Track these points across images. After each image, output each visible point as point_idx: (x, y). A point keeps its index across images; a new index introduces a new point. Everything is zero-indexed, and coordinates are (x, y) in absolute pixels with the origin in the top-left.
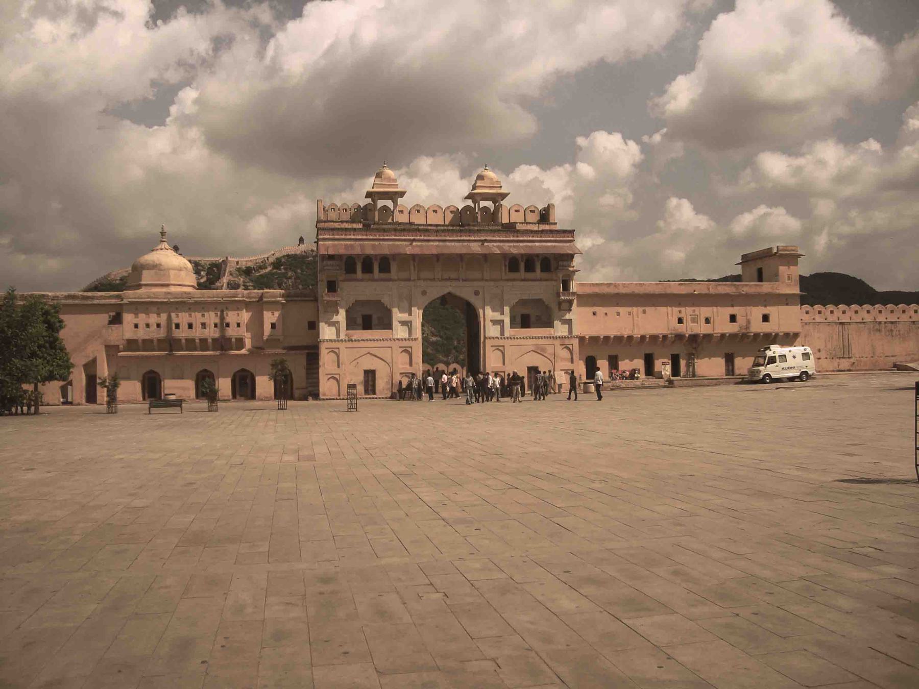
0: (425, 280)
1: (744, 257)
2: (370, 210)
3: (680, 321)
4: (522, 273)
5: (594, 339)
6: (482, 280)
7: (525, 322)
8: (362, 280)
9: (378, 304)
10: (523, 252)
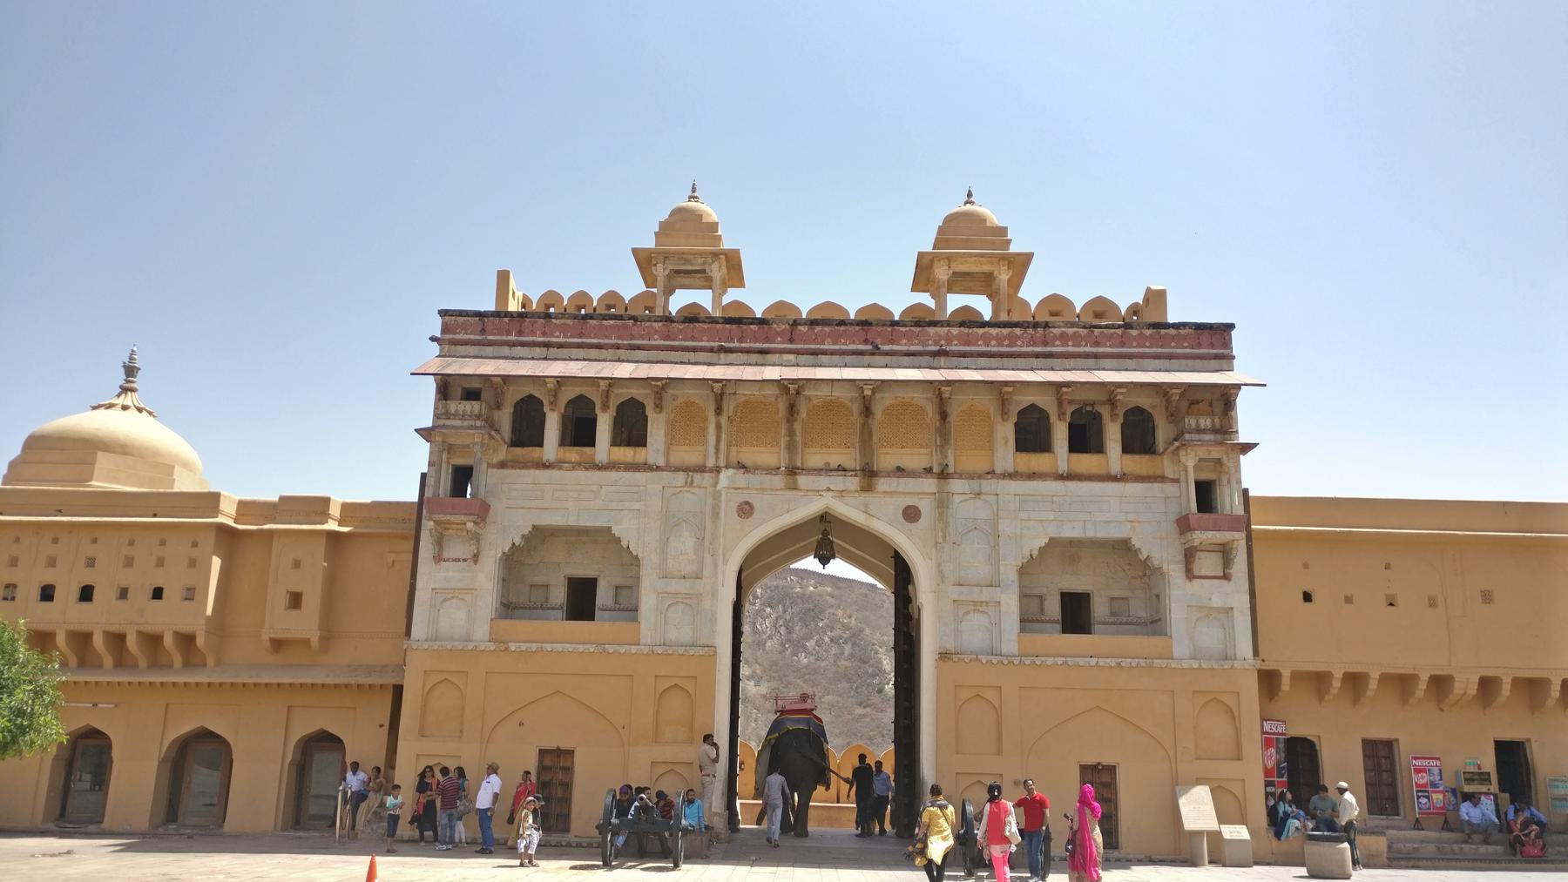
7: (1076, 614)
9: (603, 538)
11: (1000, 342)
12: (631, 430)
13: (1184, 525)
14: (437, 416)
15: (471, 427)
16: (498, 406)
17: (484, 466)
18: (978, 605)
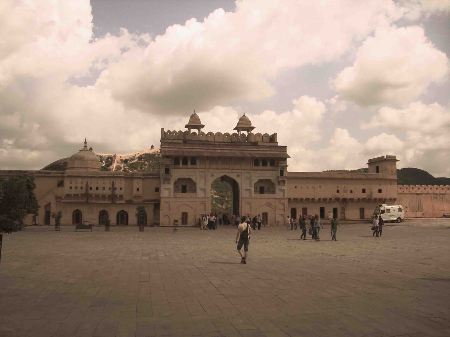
0: (213, 169)
1: (369, 160)
2: (187, 134)
3: (338, 192)
4: (261, 167)
5: (296, 200)
6: (241, 169)
7: (262, 191)
9: (190, 180)
10: (261, 156)
13: (278, 177)
18: (247, 190)
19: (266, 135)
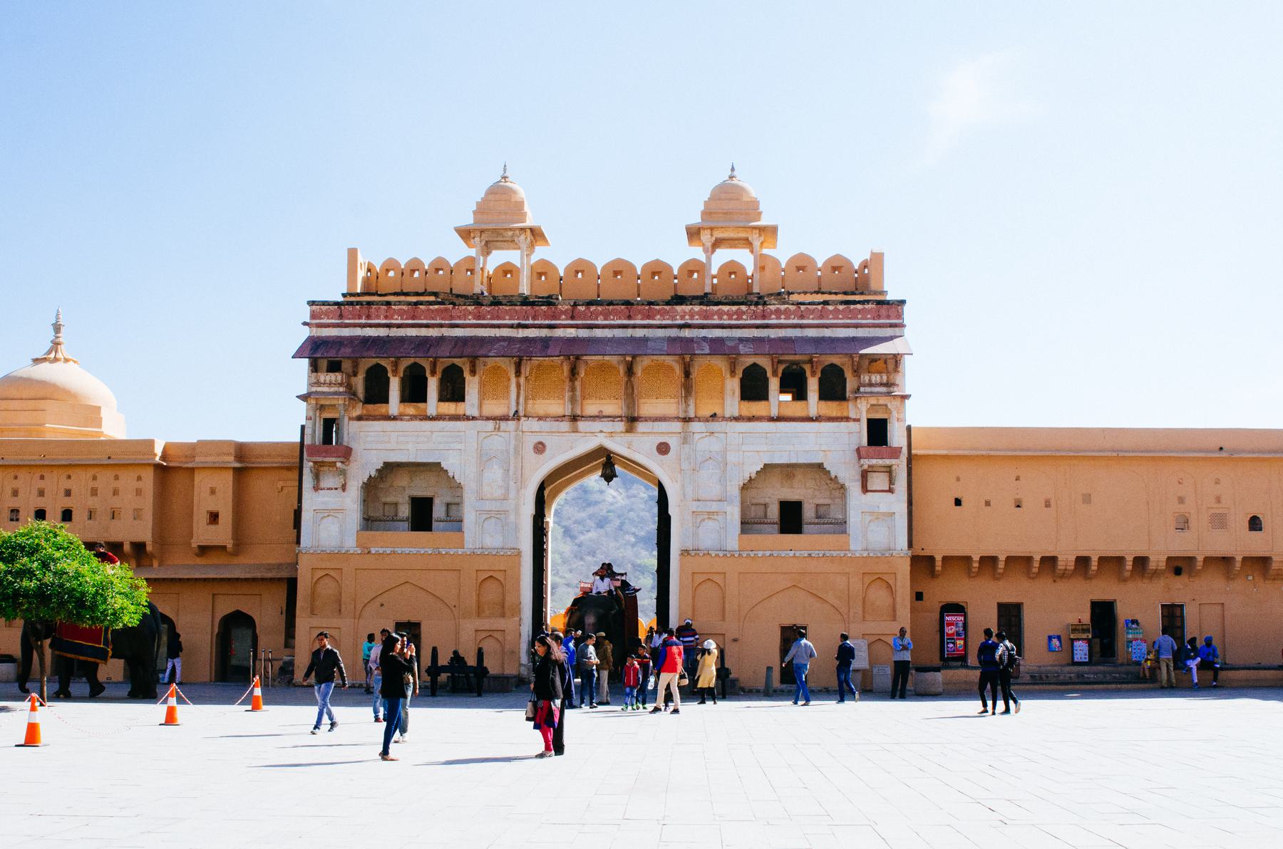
7: (791, 518)
8: (395, 418)
11: (730, 316)
12: (453, 390)
14: (311, 385)
15: (335, 393)
16: (355, 374)
17: (346, 419)
19: (837, 265)
